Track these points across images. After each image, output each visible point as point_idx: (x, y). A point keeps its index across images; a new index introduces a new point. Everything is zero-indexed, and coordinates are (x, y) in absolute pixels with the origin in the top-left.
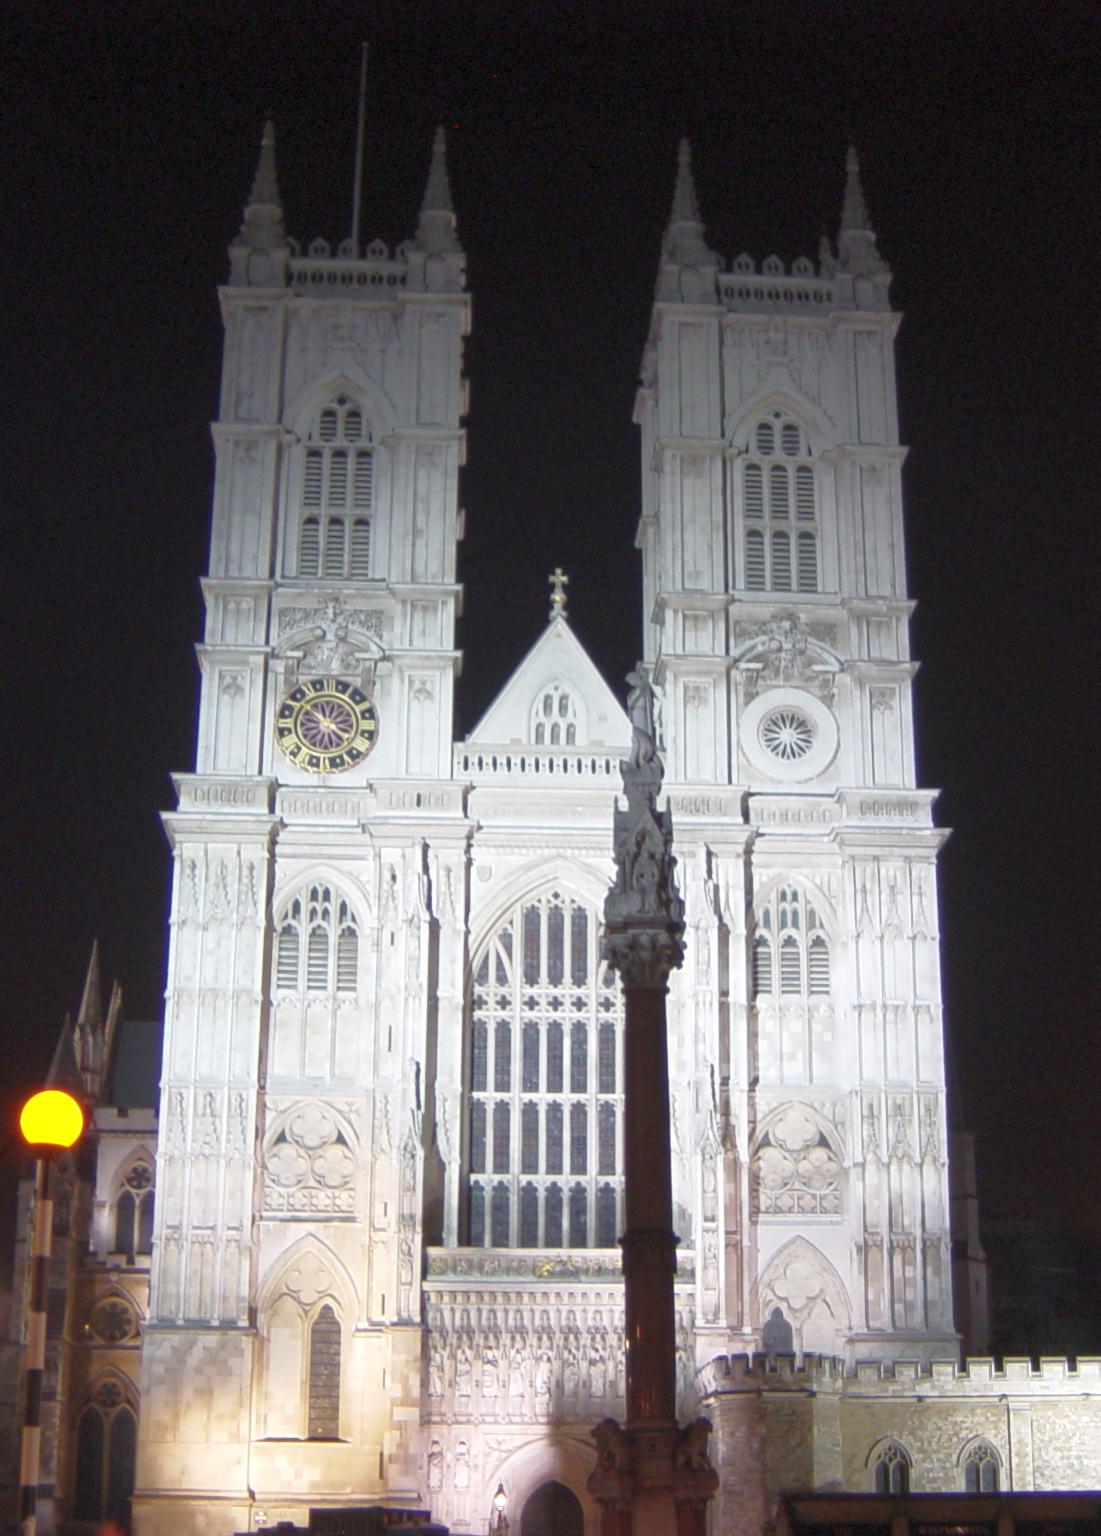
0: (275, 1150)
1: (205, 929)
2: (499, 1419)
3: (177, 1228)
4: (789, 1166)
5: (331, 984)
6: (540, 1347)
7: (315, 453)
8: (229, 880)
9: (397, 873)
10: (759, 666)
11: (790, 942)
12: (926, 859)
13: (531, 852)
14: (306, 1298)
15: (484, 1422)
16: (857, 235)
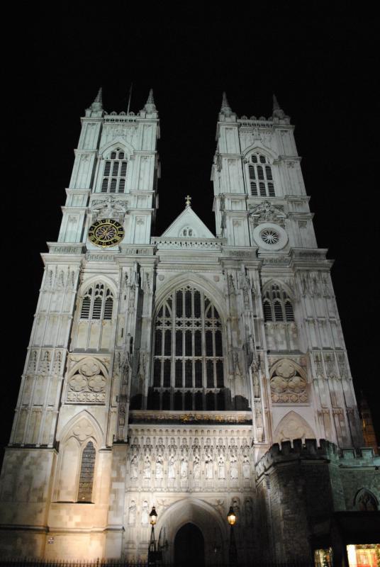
0: (73, 377)
1: (53, 293)
2: (163, 489)
3: (27, 405)
4: (285, 383)
5: (102, 317)
6: (182, 455)
7: (108, 163)
8: (64, 276)
9: (128, 275)
10: (258, 215)
11: (277, 303)
12: (327, 272)
13: (179, 271)
14: (82, 438)
15: (156, 491)
16: (278, 111)
